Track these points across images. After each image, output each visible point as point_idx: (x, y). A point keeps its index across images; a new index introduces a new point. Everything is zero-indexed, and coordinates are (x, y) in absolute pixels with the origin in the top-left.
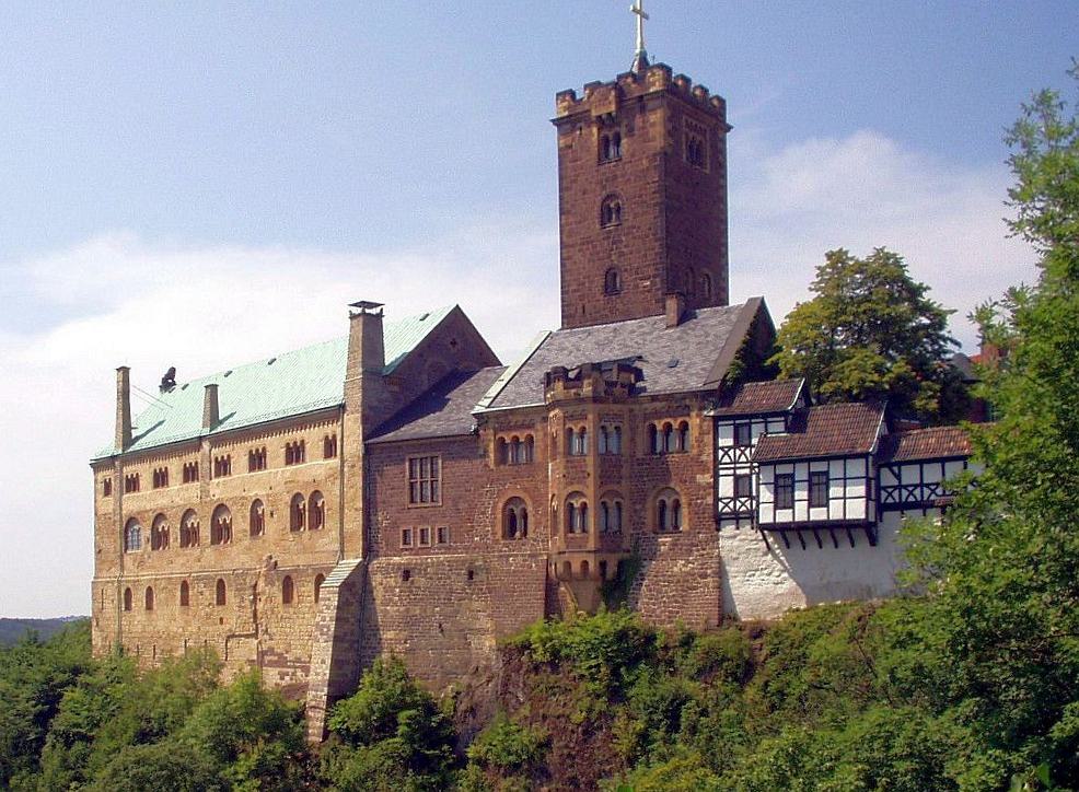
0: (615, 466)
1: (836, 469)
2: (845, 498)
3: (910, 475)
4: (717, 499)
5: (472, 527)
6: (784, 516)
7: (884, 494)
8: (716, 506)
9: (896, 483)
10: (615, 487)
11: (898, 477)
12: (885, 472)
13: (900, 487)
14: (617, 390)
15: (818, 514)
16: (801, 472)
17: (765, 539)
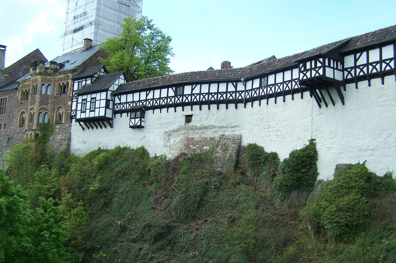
0: (46, 99)
1: (98, 96)
2: (99, 108)
3: (123, 98)
4: (72, 111)
5: (12, 123)
6: (83, 116)
7: (116, 107)
8: (71, 113)
9: (119, 102)
10: (45, 106)
11: (120, 100)
12: (116, 97)
13: (120, 104)
14: (49, 71)
15: (92, 115)
16: (89, 97)
17: (80, 125)
